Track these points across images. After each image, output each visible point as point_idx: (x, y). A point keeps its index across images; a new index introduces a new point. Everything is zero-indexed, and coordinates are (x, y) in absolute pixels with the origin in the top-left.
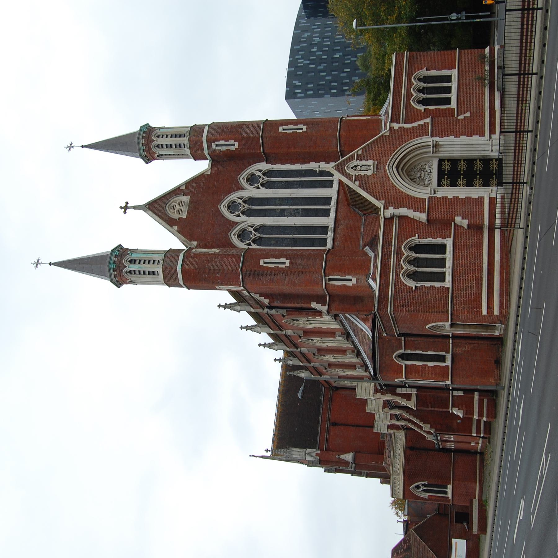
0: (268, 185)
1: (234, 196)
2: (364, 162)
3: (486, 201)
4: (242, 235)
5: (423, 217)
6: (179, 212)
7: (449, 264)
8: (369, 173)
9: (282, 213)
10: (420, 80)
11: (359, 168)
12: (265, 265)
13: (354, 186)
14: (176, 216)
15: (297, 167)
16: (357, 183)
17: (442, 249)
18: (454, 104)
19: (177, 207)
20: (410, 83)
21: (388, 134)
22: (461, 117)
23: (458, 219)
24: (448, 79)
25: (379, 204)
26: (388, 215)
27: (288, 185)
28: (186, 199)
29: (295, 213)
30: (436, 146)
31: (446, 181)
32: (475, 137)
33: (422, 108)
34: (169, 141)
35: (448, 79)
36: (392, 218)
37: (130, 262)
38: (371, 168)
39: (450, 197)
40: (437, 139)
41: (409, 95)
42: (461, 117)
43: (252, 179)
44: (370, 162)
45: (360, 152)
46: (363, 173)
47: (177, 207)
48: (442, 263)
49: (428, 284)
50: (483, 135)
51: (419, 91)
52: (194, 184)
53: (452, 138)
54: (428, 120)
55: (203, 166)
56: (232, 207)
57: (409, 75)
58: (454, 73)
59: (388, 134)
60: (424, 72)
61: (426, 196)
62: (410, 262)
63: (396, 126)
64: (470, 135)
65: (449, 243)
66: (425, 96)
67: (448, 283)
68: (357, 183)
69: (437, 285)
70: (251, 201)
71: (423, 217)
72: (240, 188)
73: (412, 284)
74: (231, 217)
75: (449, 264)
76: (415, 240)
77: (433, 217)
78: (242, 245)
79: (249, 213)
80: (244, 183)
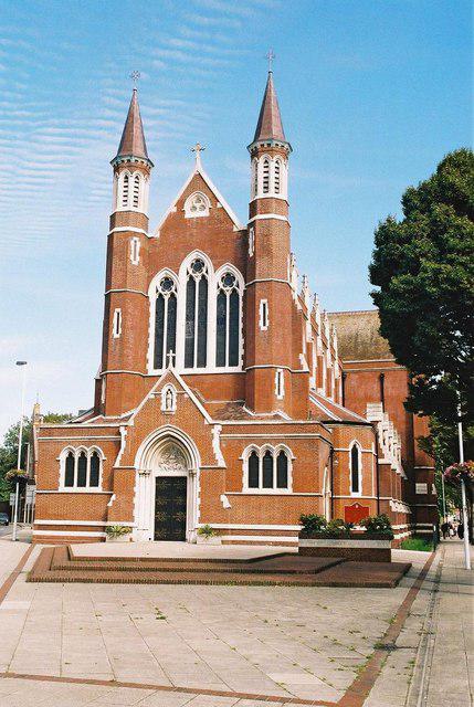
0: (221, 297)
1: (208, 264)
2: (175, 401)
3: (126, 524)
4: (167, 283)
5: (117, 465)
6: (195, 208)
7: (81, 490)
8: (163, 408)
9: (190, 317)
10: (282, 453)
11: (170, 396)
12: (116, 315)
13: (151, 396)
14: (187, 207)
15: (241, 325)
16: (153, 396)
17: (94, 483)
18: (246, 490)
19: (198, 205)
20: (277, 441)
21: (206, 423)
22: (224, 498)
23: (113, 497)
24: (282, 484)
25: (131, 423)
26: (122, 430)
27: (221, 321)
28: (205, 213)
29: (190, 332)
30: (192, 474)
31: (164, 485)
32: (198, 514)
33: (245, 456)
34: (272, 175)
35: (282, 484)
36: (119, 434)
37: (126, 177)
38: (169, 409)
39: (135, 489)
40: (198, 474)
41: (261, 442)
42: (224, 498)
43: (228, 279)
44: (175, 407)
45: (186, 396)
46: (163, 401)
47: (198, 205)
48: (82, 483)
49: (62, 471)
50: (201, 521)
51: (268, 454)
52: (222, 217)
53: (199, 490)
54: (222, 463)
55: (240, 221)
56: (198, 265)
57: (287, 440)
58: (289, 491)
59: (206, 423)
60: (290, 456)
61: (136, 466)
62: (83, 454)
63: (216, 430)
64: (201, 509)
65: (99, 489)
66: (261, 460)
67: (62, 488)
68: (153, 396)
69: (62, 480)
70: (204, 281)
71: (117, 465)
72: (216, 267)
73: (63, 457)
74: (186, 265)
75: (81, 490)
76: (102, 457)
77: (116, 473)
78: (156, 282)
79: (191, 282)
80: (223, 270)
